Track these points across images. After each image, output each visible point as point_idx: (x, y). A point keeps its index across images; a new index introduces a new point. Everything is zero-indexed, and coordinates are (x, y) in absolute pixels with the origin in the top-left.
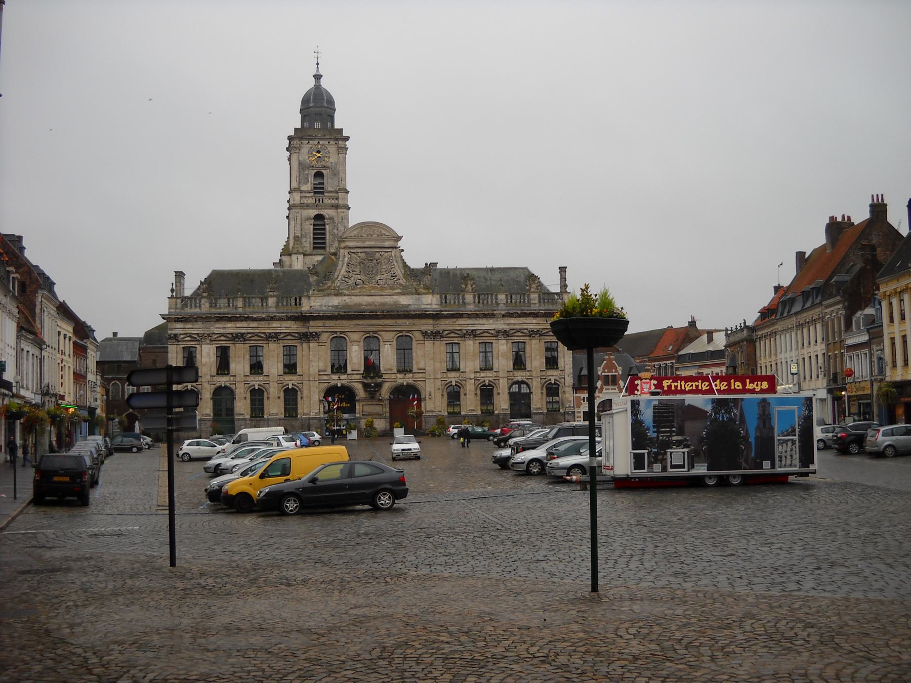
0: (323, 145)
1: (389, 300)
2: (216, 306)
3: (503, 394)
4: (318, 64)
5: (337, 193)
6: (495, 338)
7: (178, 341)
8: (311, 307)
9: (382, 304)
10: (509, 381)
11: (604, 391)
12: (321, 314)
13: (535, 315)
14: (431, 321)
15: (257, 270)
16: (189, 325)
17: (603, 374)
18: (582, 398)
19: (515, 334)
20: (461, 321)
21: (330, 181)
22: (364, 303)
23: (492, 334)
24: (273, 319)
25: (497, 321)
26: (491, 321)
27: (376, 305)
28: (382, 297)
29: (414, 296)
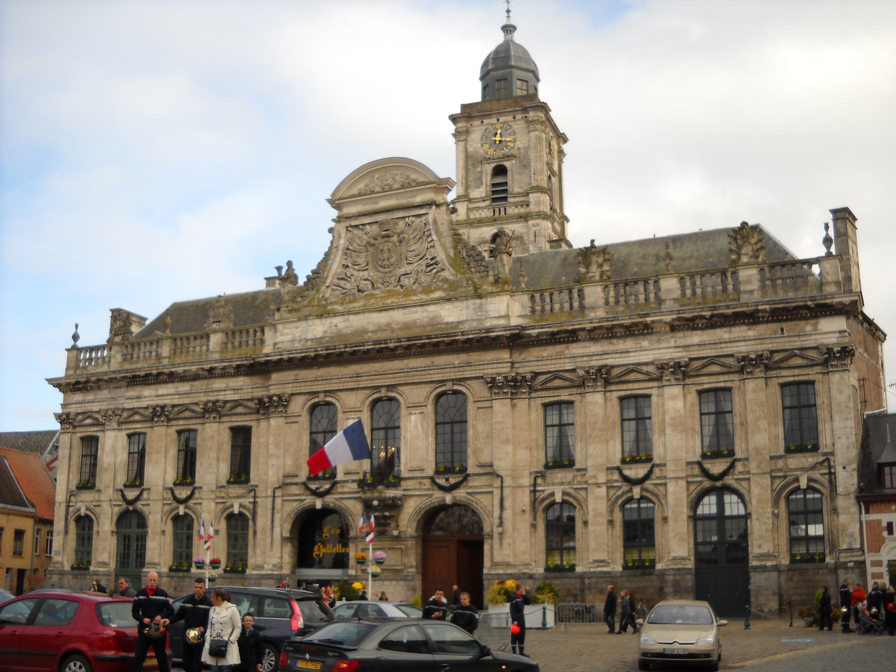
0: (504, 123)
1: (419, 315)
2: (132, 358)
3: (676, 520)
4: (508, 11)
5: (528, 194)
6: (655, 384)
7: (74, 427)
8: (275, 344)
9: (406, 326)
10: (692, 487)
12: (285, 357)
13: (751, 318)
14: (505, 355)
15: (247, 294)
16: (90, 397)
18: (884, 524)
19: (705, 371)
20: (576, 349)
21: (516, 177)
22: (371, 328)
23: (647, 373)
24: (211, 373)
25: (659, 341)
26: (645, 343)
27: (393, 330)
28: (407, 310)
29: (471, 302)
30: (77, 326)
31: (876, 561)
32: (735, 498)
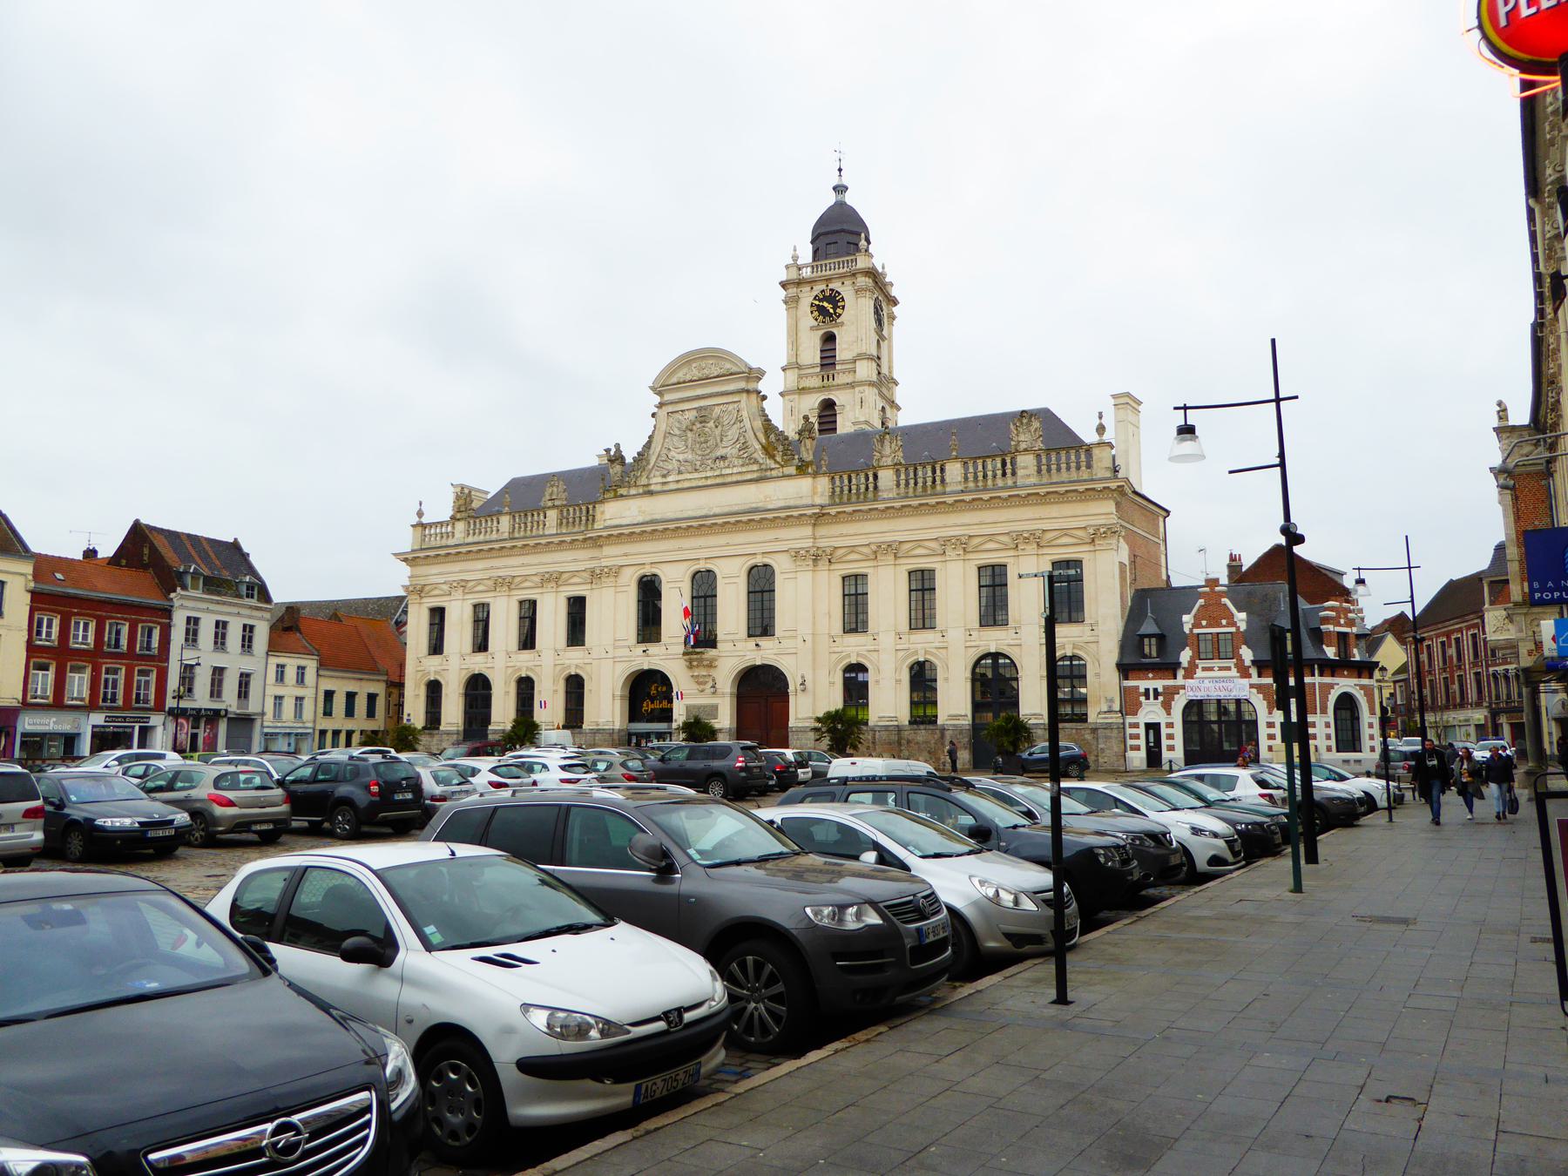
4: (840, 170)
11: (1199, 673)
14: (808, 531)
17: (1196, 631)
30: (421, 504)
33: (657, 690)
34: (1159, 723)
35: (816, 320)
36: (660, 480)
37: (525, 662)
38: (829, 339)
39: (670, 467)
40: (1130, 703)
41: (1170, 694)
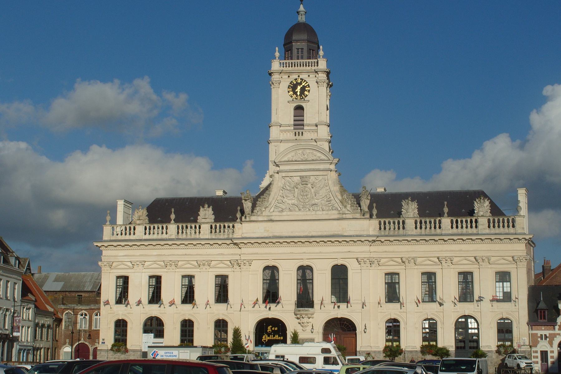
18: (539, 335)
31: (535, 351)
32: (473, 320)
33: (272, 329)
34: (547, 351)
35: (292, 97)
36: (278, 214)
37: (187, 312)
38: (299, 109)
39: (284, 207)
40: (534, 342)
41: (552, 337)
